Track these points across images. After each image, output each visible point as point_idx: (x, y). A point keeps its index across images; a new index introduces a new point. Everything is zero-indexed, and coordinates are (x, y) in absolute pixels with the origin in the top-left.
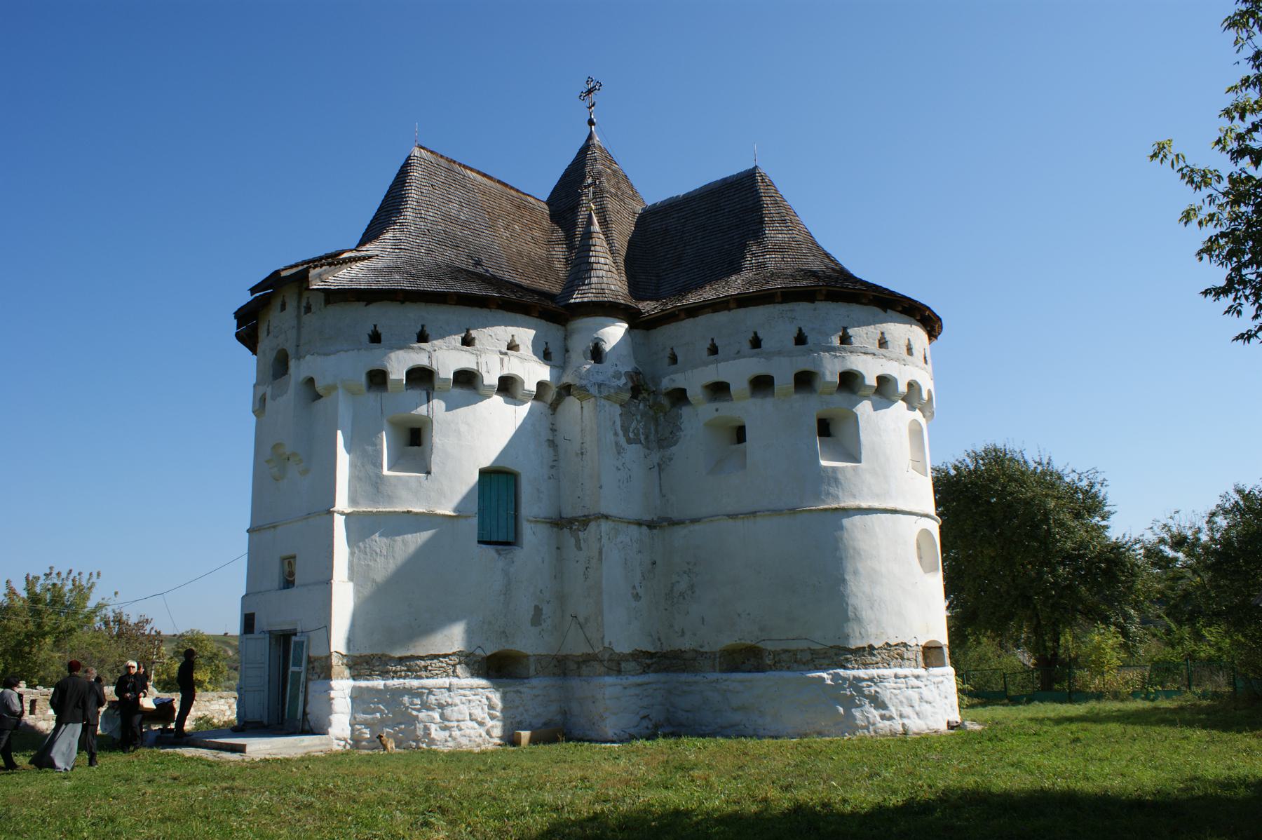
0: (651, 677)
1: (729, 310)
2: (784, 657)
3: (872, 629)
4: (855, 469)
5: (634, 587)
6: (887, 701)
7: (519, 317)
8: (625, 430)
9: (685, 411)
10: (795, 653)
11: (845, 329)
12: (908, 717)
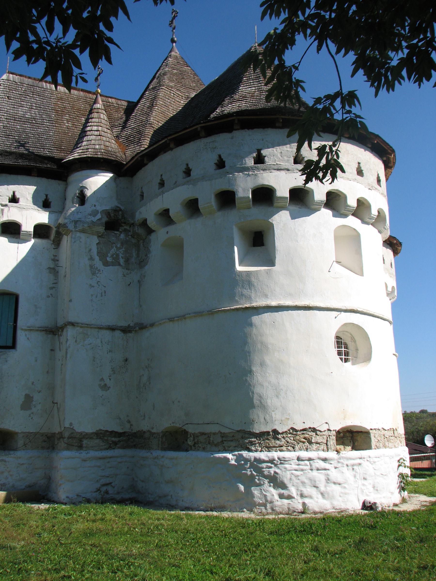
0: (117, 452)
1: (172, 149)
3: (277, 415)
4: (267, 272)
5: (102, 379)
6: (286, 481)
7: (20, 177)
8: (102, 256)
9: (153, 236)
10: (208, 435)
11: (259, 151)
12: (311, 497)
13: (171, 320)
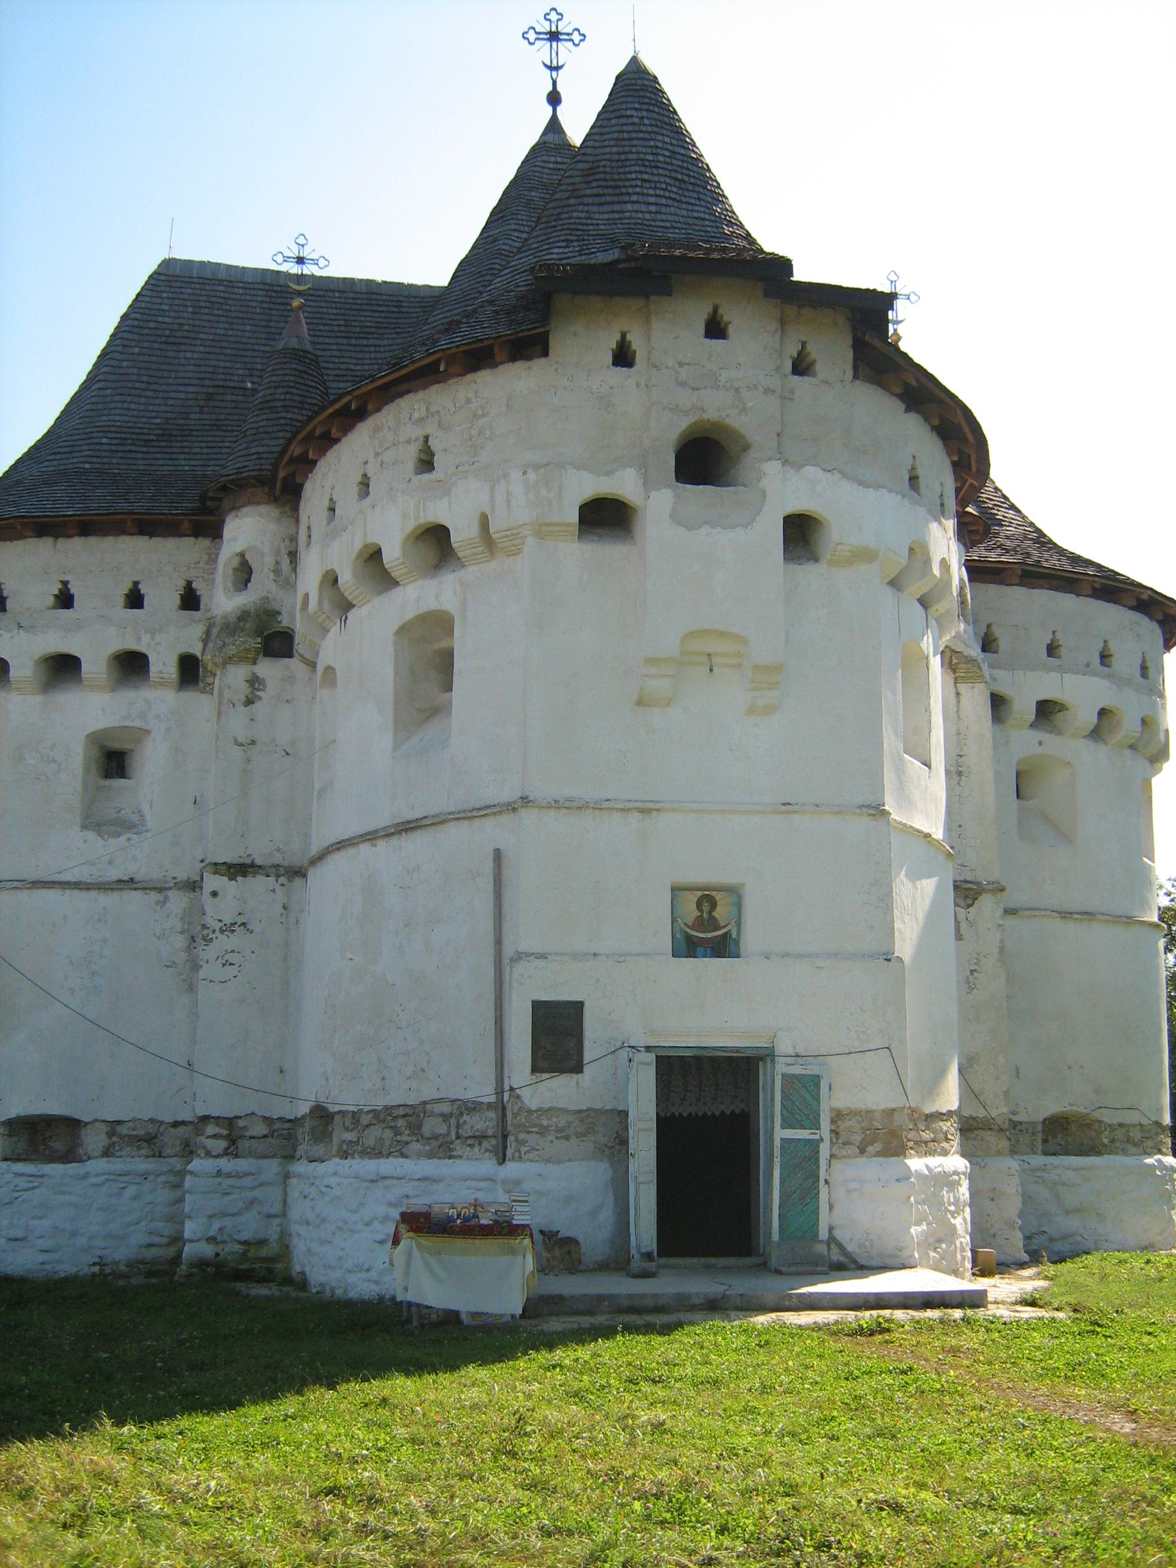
2: (1119, 1134)
13: (1066, 915)
